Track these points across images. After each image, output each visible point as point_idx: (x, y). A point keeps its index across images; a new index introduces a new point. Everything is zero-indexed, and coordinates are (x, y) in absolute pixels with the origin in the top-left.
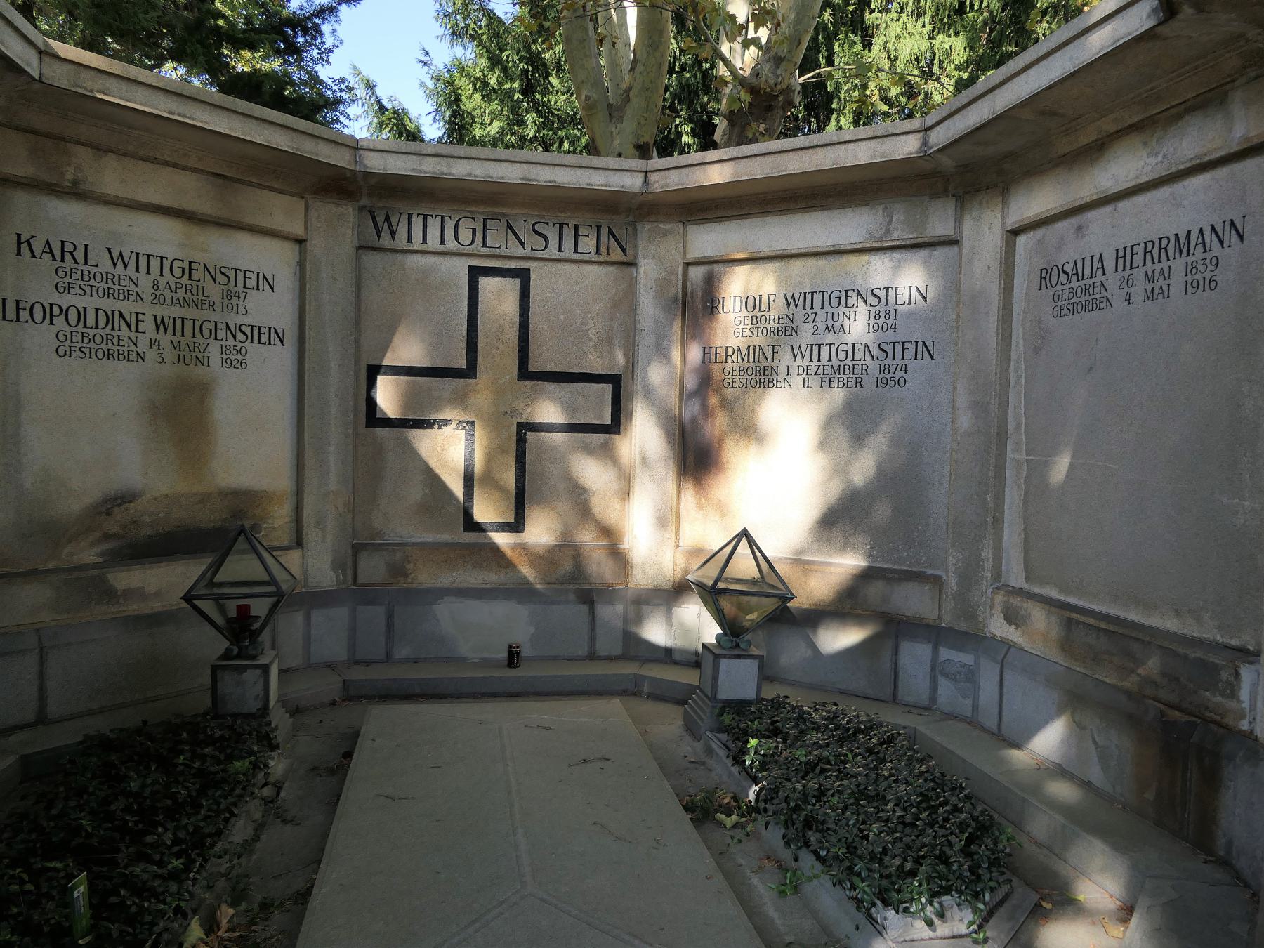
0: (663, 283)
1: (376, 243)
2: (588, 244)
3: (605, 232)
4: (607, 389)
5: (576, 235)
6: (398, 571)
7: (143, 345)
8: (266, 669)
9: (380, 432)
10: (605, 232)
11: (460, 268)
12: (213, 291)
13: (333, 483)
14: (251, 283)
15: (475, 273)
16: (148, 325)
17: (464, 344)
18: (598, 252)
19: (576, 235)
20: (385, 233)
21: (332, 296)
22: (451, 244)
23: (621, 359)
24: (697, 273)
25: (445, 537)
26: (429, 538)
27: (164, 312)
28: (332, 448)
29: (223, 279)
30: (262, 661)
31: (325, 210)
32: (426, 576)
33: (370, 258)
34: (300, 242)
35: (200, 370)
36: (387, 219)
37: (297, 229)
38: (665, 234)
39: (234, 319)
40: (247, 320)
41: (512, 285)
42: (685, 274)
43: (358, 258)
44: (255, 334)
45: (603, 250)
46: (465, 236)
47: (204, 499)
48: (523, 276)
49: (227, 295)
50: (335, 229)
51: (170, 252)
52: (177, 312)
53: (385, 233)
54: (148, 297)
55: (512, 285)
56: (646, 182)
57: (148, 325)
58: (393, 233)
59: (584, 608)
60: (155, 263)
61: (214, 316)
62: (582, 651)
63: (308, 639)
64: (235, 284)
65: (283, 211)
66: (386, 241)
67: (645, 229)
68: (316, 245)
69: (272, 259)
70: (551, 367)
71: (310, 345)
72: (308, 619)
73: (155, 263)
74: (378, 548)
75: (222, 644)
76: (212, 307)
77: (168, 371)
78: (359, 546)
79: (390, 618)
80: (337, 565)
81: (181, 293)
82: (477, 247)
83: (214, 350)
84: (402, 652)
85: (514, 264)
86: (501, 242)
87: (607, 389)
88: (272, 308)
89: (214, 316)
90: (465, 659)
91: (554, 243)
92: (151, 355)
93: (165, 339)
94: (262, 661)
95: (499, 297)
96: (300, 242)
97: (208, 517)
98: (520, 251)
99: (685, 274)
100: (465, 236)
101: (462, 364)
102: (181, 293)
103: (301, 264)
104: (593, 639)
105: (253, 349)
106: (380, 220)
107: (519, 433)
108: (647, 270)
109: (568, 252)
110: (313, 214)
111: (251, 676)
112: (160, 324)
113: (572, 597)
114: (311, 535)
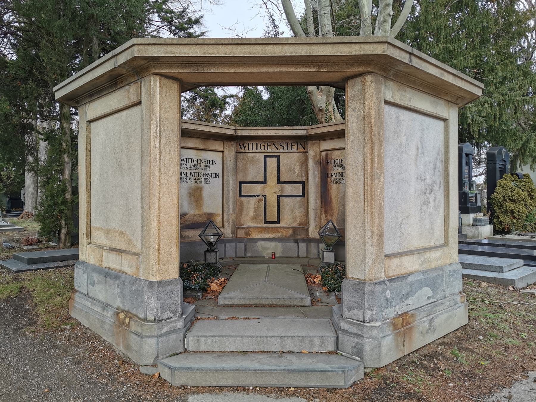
0: (315, 157)
1: (240, 151)
2: (294, 147)
3: (299, 144)
5: (291, 146)
6: (247, 234)
7: (188, 180)
8: (216, 252)
10: (299, 144)
11: (262, 155)
12: (203, 165)
14: (211, 163)
15: (265, 157)
16: (189, 175)
19: (291, 146)
20: (243, 148)
21: (230, 164)
22: (259, 150)
23: (304, 178)
24: (323, 154)
25: (259, 225)
26: (255, 225)
27: (192, 171)
29: (204, 162)
31: (228, 144)
32: (255, 235)
33: (239, 155)
34: (222, 152)
35: (200, 185)
36: (243, 145)
37: (222, 149)
38: (315, 144)
39: (207, 172)
41: (275, 159)
42: (320, 154)
43: (236, 155)
45: (299, 149)
46: (263, 147)
47: (201, 215)
48: (278, 157)
49: (206, 166)
50: (230, 150)
51: (193, 157)
52: (195, 171)
53: (243, 148)
54: (189, 168)
55: (275, 159)
56: (307, 132)
57: (189, 175)
58: (245, 148)
60: (190, 160)
61: (203, 172)
63: (225, 251)
64: (207, 163)
65: (217, 145)
66: (243, 150)
67: (310, 143)
68: (226, 152)
69: (216, 157)
70: (286, 180)
71: (225, 177)
72: (225, 246)
73: (190, 160)
74: (242, 228)
76: (202, 169)
77: (193, 185)
78: (237, 227)
79: (245, 246)
80: (232, 232)
81: (196, 167)
83: (203, 179)
84: (249, 255)
85: (275, 154)
86: (272, 148)
88: (216, 169)
89: (203, 172)
91: (285, 148)
92: (190, 182)
93: (192, 178)
95: (272, 162)
96: (222, 152)
97: (202, 220)
98: (277, 151)
99: (320, 154)
100: (263, 147)
101: (263, 180)
102: (196, 167)
103: (223, 157)
106: (241, 145)
107: (278, 198)
108: (311, 153)
109: (289, 150)
110: (225, 145)
111: (213, 254)
112: (191, 174)
113: (292, 241)
114: (226, 225)
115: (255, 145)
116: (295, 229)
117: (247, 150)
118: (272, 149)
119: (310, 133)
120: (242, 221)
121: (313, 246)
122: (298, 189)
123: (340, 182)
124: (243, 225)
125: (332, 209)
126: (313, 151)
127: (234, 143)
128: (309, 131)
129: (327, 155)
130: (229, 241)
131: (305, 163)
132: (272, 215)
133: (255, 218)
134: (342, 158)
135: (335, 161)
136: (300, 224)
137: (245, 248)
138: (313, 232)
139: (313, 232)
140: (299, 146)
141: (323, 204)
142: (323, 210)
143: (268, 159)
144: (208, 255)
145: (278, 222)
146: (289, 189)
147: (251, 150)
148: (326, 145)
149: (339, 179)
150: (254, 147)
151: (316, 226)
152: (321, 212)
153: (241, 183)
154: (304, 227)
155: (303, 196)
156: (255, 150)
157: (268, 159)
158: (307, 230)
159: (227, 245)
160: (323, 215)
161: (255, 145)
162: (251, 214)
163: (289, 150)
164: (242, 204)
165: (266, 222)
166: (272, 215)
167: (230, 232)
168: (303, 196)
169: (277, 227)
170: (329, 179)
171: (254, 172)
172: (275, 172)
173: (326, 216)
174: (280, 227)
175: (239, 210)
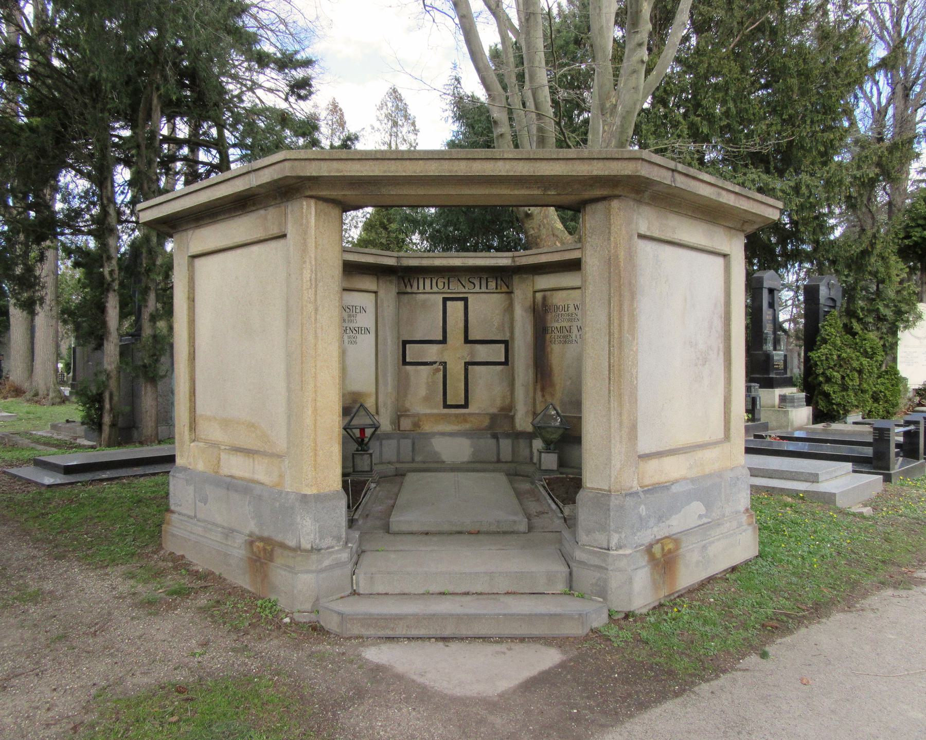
2: (492, 285)
4: (503, 346)
6: (416, 425)
8: (371, 455)
9: (408, 367)
11: (439, 298)
13: (390, 389)
15: (445, 300)
17: (441, 330)
18: (497, 288)
22: (435, 289)
24: (539, 296)
25: (435, 411)
26: (428, 411)
28: (389, 374)
30: (371, 451)
32: (427, 427)
34: (376, 292)
36: (409, 281)
37: (374, 288)
39: (352, 325)
40: (357, 325)
42: (534, 297)
44: (359, 330)
46: (441, 285)
48: (465, 300)
49: (350, 316)
55: (461, 304)
58: (411, 286)
59: (494, 441)
62: (494, 459)
65: (369, 283)
66: (409, 290)
67: (516, 279)
68: (381, 294)
70: (478, 338)
72: (381, 444)
74: (408, 416)
75: (356, 446)
78: (400, 414)
79: (413, 444)
80: (392, 423)
82: (446, 290)
84: (419, 458)
85: (461, 296)
87: (503, 346)
90: (444, 462)
94: (371, 451)
95: (456, 308)
96: (376, 292)
98: (464, 290)
99: (534, 297)
100: (441, 285)
101: (441, 338)
104: (498, 454)
105: (359, 336)
106: (406, 281)
109: (484, 289)
111: (366, 457)
114: (382, 410)
115: (428, 282)
116: (493, 417)
117: (415, 289)
118: (456, 288)
119: (518, 264)
120: (407, 405)
121: (522, 443)
122: (497, 354)
123: (565, 342)
124: (408, 410)
125: (552, 385)
126: (523, 292)
127: (394, 278)
128: (516, 259)
129: (544, 298)
130: (388, 436)
131: (510, 309)
132: (456, 395)
133: (427, 399)
134: (569, 302)
135: (558, 308)
136: (502, 409)
137: (413, 449)
138: (523, 422)
139: (523, 422)
140: (499, 282)
141: (539, 376)
142: (539, 387)
143: (449, 303)
144: (358, 461)
145: (466, 405)
146: (483, 353)
147: (421, 290)
148: (544, 282)
149: (564, 337)
150: (426, 284)
151: (527, 413)
152: (535, 390)
153: (405, 343)
154: (507, 413)
155: (506, 363)
156: (428, 289)
157: (449, 303)
158: (512, 418)
159: (384, 442)
160: (539, 393)
161: (428, 282)
162: (423, 392)
163: (484, 289)
164: (407, 375)
165: (446, 406)
166: (456, 395)
167: (388, 423)
168: (506, 363)
169: (464, 414)
170: (548, 336)
171: (427, 324)
172: (461, 325)
173: (543, 396)
174: (470, 414)
175: (403, 386)
